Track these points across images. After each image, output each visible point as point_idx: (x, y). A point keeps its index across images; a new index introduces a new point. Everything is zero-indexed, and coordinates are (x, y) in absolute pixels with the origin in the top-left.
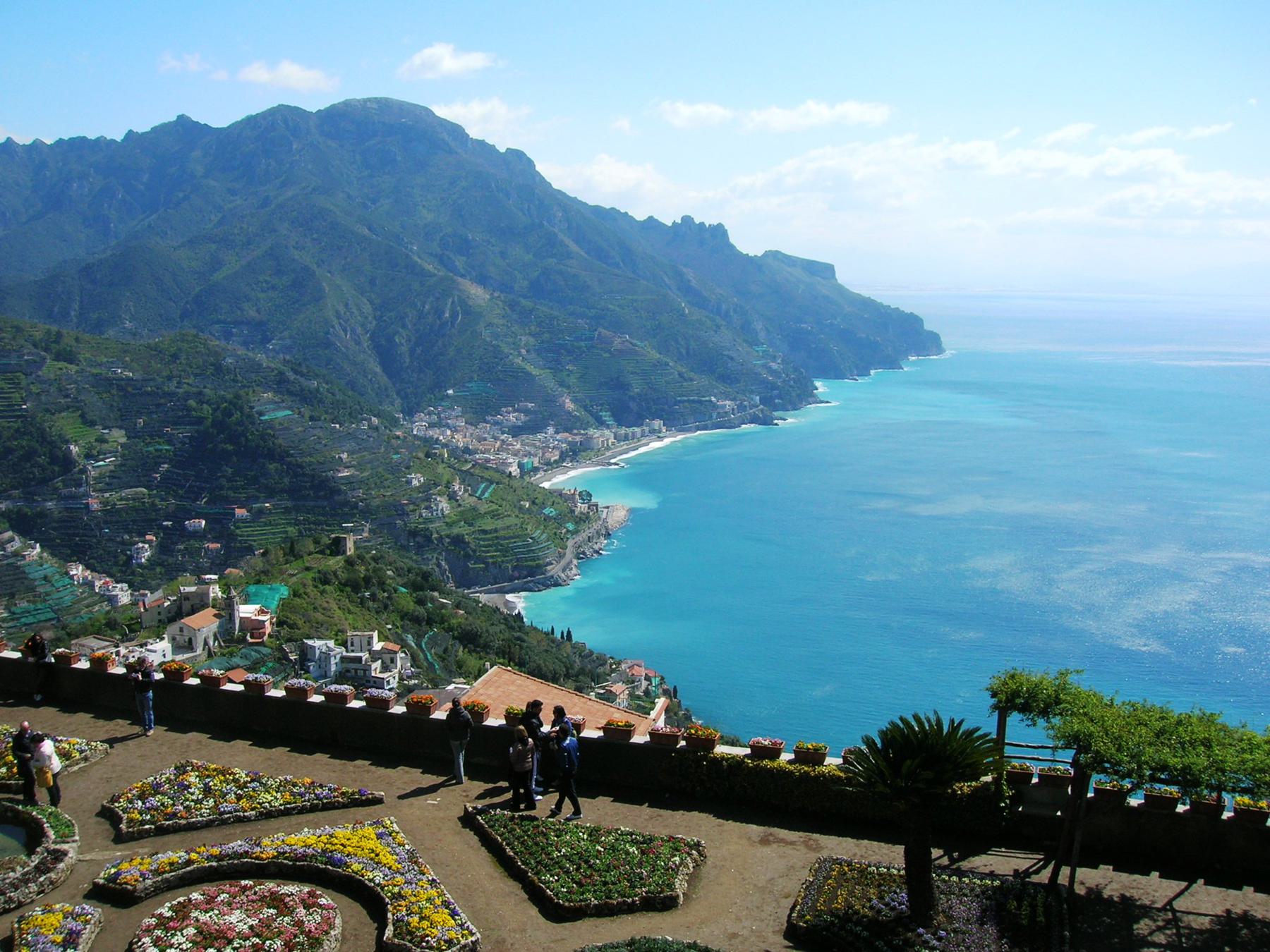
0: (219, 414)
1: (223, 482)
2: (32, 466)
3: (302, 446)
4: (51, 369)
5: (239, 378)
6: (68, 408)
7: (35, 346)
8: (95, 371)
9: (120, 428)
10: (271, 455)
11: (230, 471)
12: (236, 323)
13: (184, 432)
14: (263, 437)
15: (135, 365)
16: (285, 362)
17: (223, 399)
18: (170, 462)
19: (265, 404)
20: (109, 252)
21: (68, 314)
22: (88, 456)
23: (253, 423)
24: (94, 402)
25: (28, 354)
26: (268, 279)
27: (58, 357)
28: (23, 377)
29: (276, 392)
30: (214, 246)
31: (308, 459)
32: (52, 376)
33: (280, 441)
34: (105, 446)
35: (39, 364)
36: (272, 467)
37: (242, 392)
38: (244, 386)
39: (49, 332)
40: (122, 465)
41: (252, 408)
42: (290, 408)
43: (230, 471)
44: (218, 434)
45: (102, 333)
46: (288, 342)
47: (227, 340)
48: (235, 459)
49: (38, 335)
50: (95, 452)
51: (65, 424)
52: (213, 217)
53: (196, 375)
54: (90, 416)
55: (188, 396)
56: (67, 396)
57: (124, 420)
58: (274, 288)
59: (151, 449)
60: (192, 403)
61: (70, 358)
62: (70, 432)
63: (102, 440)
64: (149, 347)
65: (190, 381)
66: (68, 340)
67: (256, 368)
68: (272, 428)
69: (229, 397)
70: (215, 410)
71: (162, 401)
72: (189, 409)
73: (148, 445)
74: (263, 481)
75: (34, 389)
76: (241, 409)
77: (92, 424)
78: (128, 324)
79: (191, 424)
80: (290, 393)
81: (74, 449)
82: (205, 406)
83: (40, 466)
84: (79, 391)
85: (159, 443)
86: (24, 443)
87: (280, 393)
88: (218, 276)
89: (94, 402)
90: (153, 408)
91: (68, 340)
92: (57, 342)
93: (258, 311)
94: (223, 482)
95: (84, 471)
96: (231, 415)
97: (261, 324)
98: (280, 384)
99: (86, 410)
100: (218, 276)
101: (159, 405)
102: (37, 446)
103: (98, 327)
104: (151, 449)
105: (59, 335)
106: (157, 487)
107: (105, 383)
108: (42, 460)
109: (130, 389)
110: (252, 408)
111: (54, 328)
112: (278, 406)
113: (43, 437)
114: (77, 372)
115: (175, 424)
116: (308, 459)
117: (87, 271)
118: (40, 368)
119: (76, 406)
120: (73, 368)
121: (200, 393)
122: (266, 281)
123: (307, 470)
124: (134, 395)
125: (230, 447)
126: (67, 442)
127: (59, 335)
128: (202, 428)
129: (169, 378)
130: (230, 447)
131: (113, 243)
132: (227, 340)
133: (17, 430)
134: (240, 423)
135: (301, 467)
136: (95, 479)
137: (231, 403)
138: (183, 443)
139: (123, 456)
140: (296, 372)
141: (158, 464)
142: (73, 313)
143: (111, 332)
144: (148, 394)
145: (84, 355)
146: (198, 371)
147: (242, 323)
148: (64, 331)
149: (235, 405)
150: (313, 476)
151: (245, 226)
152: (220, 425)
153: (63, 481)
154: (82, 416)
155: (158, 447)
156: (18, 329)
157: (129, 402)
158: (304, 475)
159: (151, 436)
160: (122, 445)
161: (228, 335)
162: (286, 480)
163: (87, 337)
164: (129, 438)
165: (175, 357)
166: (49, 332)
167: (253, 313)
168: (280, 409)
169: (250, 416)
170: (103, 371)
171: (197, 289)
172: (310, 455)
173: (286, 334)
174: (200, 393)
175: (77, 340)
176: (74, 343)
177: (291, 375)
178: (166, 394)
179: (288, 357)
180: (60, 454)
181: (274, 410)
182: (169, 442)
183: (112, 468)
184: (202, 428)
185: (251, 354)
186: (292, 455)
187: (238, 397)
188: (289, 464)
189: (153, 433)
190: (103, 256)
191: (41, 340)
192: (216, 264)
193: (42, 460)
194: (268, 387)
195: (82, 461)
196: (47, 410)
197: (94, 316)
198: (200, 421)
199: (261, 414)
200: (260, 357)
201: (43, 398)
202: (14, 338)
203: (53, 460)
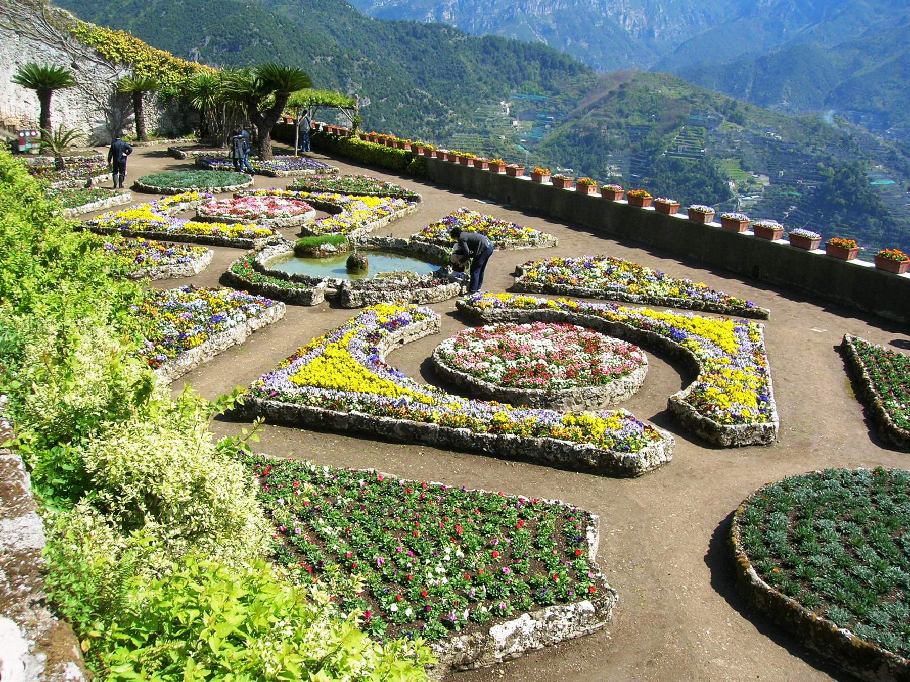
0: (839, 175)
1: (833, 225)
2: (701, 192)
3: (898, 209)
4: (726, 126)
5: (860, 151)
6: (732, 155)
7: (717, 109)
8: (755, 132)
9: (767, 175)
10: (873, 212)
11: (840, 218)
12: (865, 111)
13: (811, 186)
14: (869, 197)
15: (785, 132)
16: (897, 145)
17: (845, 165)
18: (798, 205)
19: (876, 173)
20: (779, 49)
21: (744, 90)
22: (740, 191)
23: (864, 186)
24: (749, 152)
25: (712, 115)
26: (896, 80)
27: (731, 119)
28: (704, 129)
29: (886, 166)
30: (858, 52)
31: (900, 220)
32: (725, 132)
33: (881, 202)
34: (753, 186)
35: (718, 122)
36: (872, 221)
37: (860, 162)
38: (862, 158)
39: (728, 101)
40: (763, 201)
41: (865, 175)
42: (894, 179)
43: (840, 218)
44: (836, 190)
45: (764, 107)
46: (902, 130)
47: (857, 122)
48: (845, 210)
49: (720, 102)
50: (745, 190)
51: (728, 166)
52: (860, 29)
53: (828, 145)
54: (746, 164)
55: (819, 159)
56: (733, 147)
57: (770, 170)
58: (899, 87)
59: (785, 193)
60: (821, 165)
61: (739, 121)
62: (730, 173)
63: (752, 182)
64: (797, 120)
65: (823, 149)
66: (740, 109)
67: (875, 146)
68: (877, 192)
69: (850, 164)
70: (837, 172)
71: (800, 160)
72: (818, 169)
73: (784, 190)
74: (863, 230)
75: (711, 139)
76: (857, 175)
77: (747, 169)
78: (785, 103)
79: (818, 180)
80: (897, 169)
81: (732, 185)
82: (830, 168)
83: (707, 193)
84: (741, 145)
85: (792, 190)
86: (698, 176)
87: (890, 167)
88: (858, 74)
89: (749, 152)
90: (792, 165)
91: (740, 109)
92: (732, 109)
93: (884, 104)
94: (833, 225)
95: (735, 201)
96: (848, 177)
97: (884, 114)
98: (891, 160)
99: (744, 159)
100: (858, 74)
101: (797, 163)
102: (707, 179)
103: (764, 102)
104: (785, 193)
105: (734, 104)
106: (785, 221)
107: (760, 142)
108: (708, 189)
109: (778, 148)
110: (865, 175)
111: (732, 99)
112: (885, 176)
113: (711, 174)
114: (743, 131)
115: (807, 178)
116: (900, 220)
117: (761, 61)
118: (717, 125)
119: (738, 155)
120: (740, 128)
121: (829, 158)
122: (893, 82)
123: (899, 228)
124: (780, 153)
125: (843, 201)
126: (728, 179)
127: (734, 104)
128: (825, 184)
129: (808, 145)
130: (843, 201)
131: (783, 43)
132: (857, 122)
133: (695, 166)
134: (853, 185)
135: (894, 225)
136: (742, 208)
137: (850, 168)
138: (810, 193)
139: (765, 195)
140: (904, 153)
141: (789, 205)
142: (747, 91)
143: (772, 107)
144: (791, 154)
145: (750, 120)
146: (829, 142)
147: (870, 111)
148: (739, 102)
149: (852, 171)
150: (902, 233)
151: (884, 38)
152: (839, 184)
153: (720, 206)
154: (741, 163)
155: (791, 193)
156: (707, 97)
157: (775, 157)
158: (895, 231)
159: (787, 184)
160: (766, 188)
161: (857, 120)
162: (881, 232)
163: (754, 107)
164: (771, 183)
165: (815, 129)
166: (728, 101)
167: (879, 105)
168: (886, 178)
169: (862, 181)
170: (762, 133)
171: (840, 82)
172: (903, 217)
173: (902, 124)
174: (829, 158)
175: (746, 109)
176: (744, 111)
177: (900, 155)
178: (803, 156)
179: (900, 141)
180: (720, 186)
181: (881, 179)
182: (799, 191)
183: (756, 202)
184: (825, 184)
185: (872, 135)
186: (889, 215)
187: (856, 165)
188: (885, 221)
189: (789, 182)
190: (774, 52)
191: (721, 106)
192: (857, 64)
193: (708, 189)
194: (880, 161)
195: (736, 195)
196: (718, 156)
197: (762, 94)
198: (824, 178)
199: (871, 180)
200: (879, 139)
201: (716, 147)
202: (703, 102)
203: (716, 191)
